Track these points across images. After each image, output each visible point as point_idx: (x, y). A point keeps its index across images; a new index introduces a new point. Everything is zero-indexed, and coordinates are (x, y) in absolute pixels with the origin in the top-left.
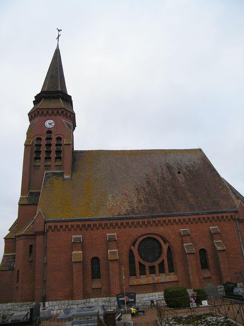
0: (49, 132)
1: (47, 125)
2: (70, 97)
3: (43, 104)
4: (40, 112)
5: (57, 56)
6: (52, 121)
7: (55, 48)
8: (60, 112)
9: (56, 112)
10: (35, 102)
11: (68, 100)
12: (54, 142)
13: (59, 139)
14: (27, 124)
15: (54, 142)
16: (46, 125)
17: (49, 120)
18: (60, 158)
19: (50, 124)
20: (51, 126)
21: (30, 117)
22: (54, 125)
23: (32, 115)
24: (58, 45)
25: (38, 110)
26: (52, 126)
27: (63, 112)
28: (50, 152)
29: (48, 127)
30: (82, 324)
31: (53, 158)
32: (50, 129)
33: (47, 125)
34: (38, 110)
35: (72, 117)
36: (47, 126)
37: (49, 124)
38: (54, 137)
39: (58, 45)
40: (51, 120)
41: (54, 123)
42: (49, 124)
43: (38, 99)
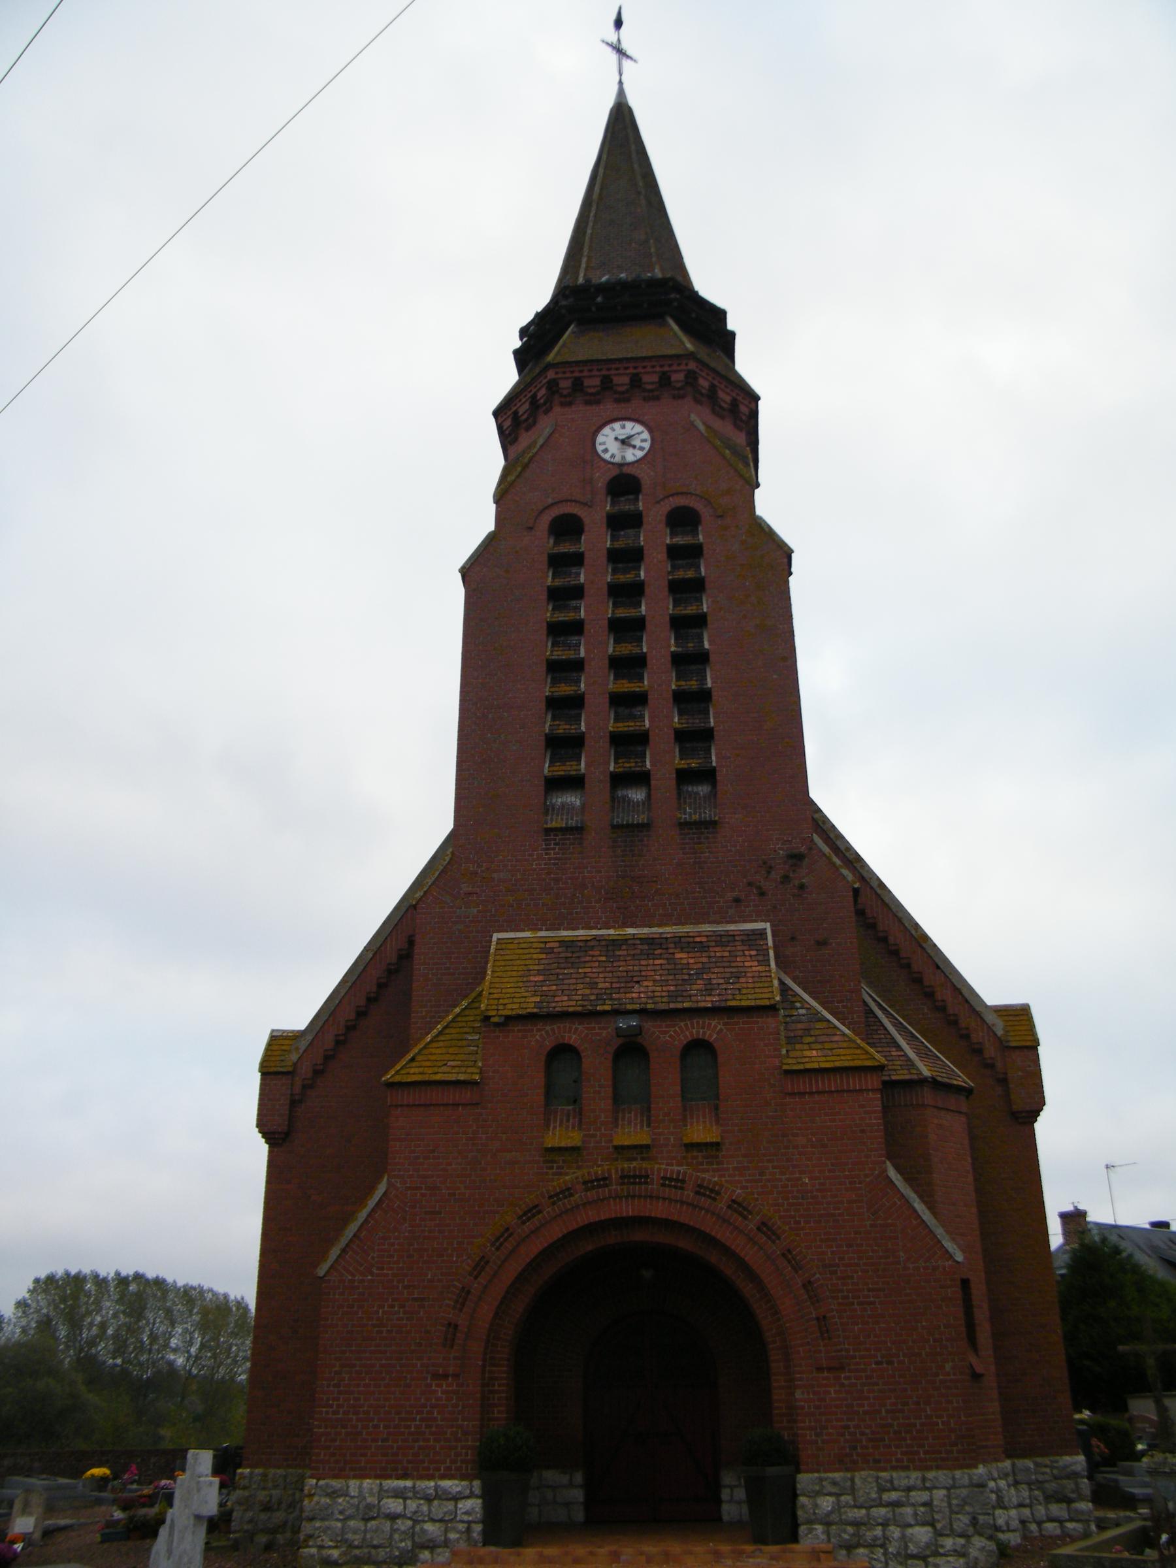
0: (624, 483)
1: (606, 451)
2: (732, 335)
3: (572, 346)
4: (565, 384)
5: (622, 129)
6: (632, 428)
7: (609, 102)
8: (678, 377)
9: (655, 378)
10: (521, 357)
11: (711, 328)
12: (654, 538)
13: (683, 519)
14: (491, 460)
15: (654, 538)
16: (600, 448)
17: (617, 425)
18: (708, 775)
19: (625, 442)
20: (631, 455)
21: (508, 423)
22: (647, 445)
23: (512, 418)
24: (620, 83)
25: (551, 374)
26: (640, 454)
27: (691, 378)
28: (638, 625)
29: (618, 459)
30: (834, 864)
31: (663, 780)
32: (626, 470)
33: (606, 451)
34: (551, 374)
35: (741, 407)
36: (607, 456)
37: (621, 441)
38: (654, 513)
39: (620, 83)
40: (629, 425)
41: (649, 442)
42: (621, 441)
43: (537, 342)
